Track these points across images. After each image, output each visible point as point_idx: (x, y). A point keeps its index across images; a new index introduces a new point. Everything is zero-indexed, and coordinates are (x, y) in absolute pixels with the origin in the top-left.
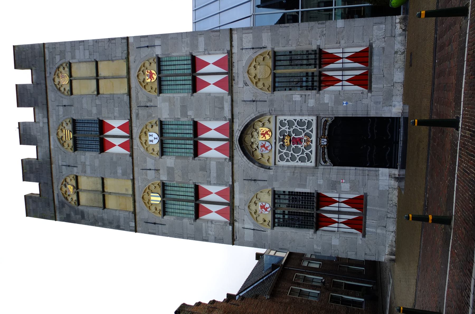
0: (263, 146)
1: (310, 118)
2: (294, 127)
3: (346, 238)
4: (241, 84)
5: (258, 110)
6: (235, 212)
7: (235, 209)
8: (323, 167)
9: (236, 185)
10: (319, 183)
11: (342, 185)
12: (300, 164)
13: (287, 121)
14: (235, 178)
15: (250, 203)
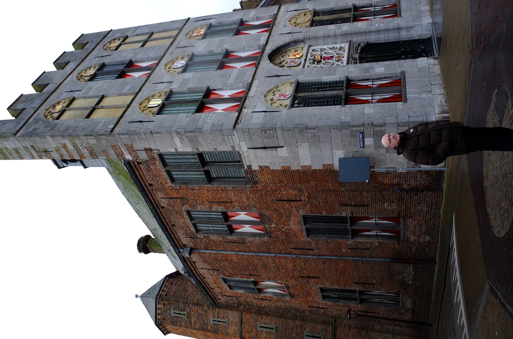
0: (293, 62)
1: (343, 45)
2: (326, 51)
3: (382, 106)
5: (293, 37)
6: (247, 101)
7: (247, 98)
9: (255, 83)
10: (350, 70)
11: (375, 69)
13: (320, 49)
14: (256, 77)
15: (267, 93)
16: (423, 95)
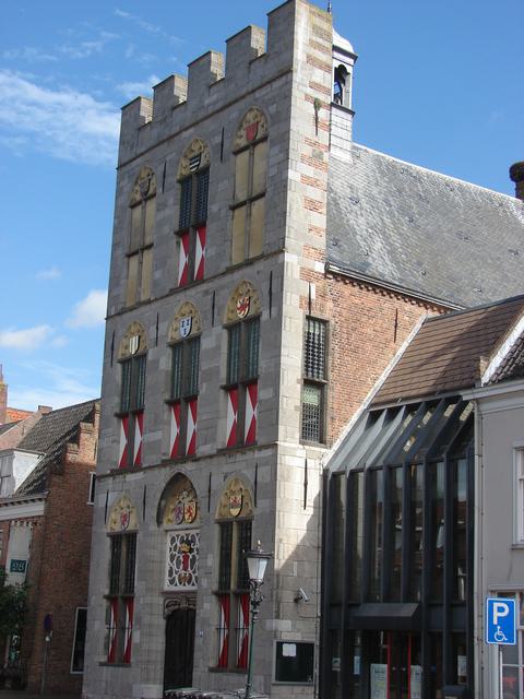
4: (226, 469)
8: (161, 603)
12: (168, 568)
16: (104, 684)
